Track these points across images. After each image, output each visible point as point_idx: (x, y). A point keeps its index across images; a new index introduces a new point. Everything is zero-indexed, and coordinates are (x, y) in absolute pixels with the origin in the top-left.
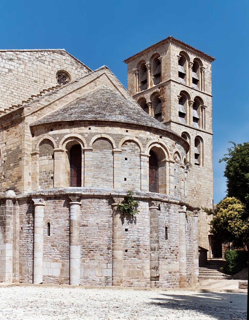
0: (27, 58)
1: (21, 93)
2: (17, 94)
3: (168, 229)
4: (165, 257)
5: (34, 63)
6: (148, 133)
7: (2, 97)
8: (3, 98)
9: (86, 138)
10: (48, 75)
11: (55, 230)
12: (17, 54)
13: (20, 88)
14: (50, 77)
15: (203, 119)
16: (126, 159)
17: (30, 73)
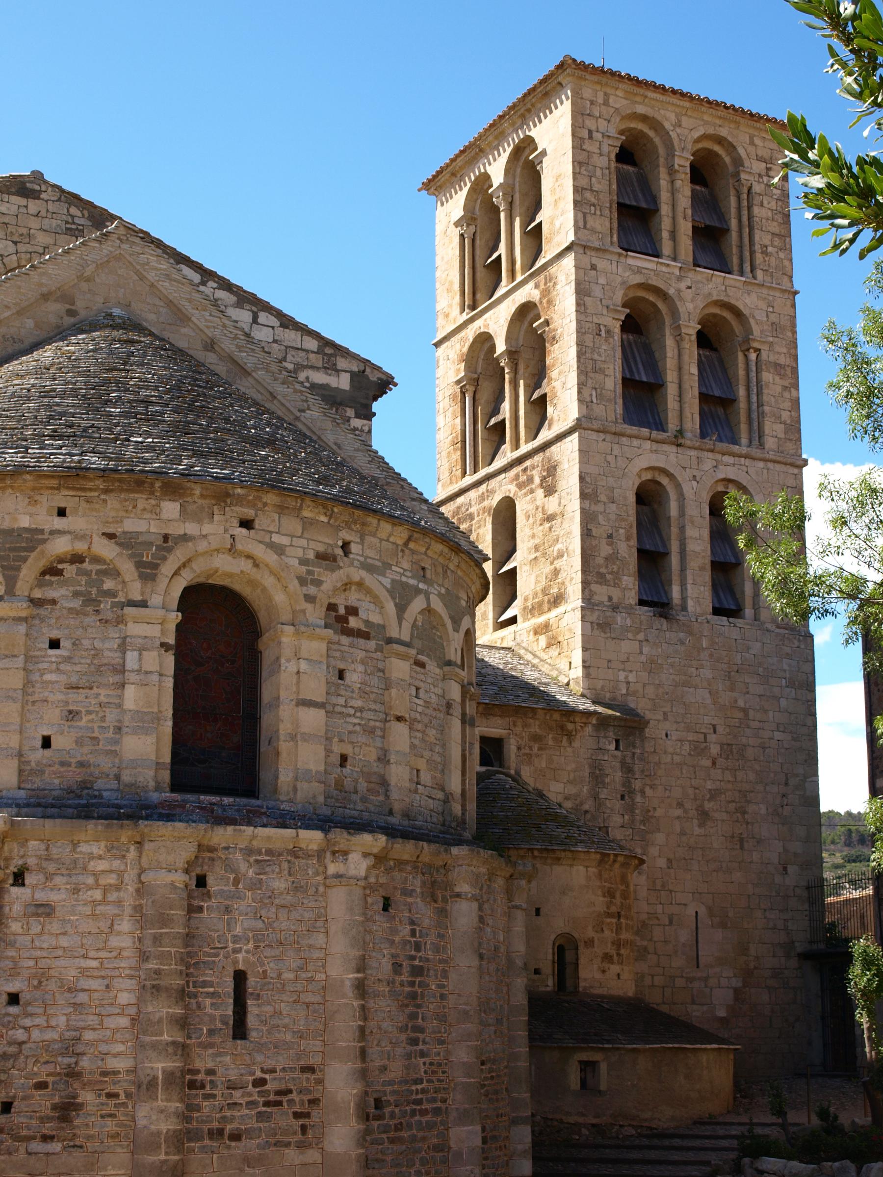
3: (252, 982)
6: (171, 508)
15: (754, 398)
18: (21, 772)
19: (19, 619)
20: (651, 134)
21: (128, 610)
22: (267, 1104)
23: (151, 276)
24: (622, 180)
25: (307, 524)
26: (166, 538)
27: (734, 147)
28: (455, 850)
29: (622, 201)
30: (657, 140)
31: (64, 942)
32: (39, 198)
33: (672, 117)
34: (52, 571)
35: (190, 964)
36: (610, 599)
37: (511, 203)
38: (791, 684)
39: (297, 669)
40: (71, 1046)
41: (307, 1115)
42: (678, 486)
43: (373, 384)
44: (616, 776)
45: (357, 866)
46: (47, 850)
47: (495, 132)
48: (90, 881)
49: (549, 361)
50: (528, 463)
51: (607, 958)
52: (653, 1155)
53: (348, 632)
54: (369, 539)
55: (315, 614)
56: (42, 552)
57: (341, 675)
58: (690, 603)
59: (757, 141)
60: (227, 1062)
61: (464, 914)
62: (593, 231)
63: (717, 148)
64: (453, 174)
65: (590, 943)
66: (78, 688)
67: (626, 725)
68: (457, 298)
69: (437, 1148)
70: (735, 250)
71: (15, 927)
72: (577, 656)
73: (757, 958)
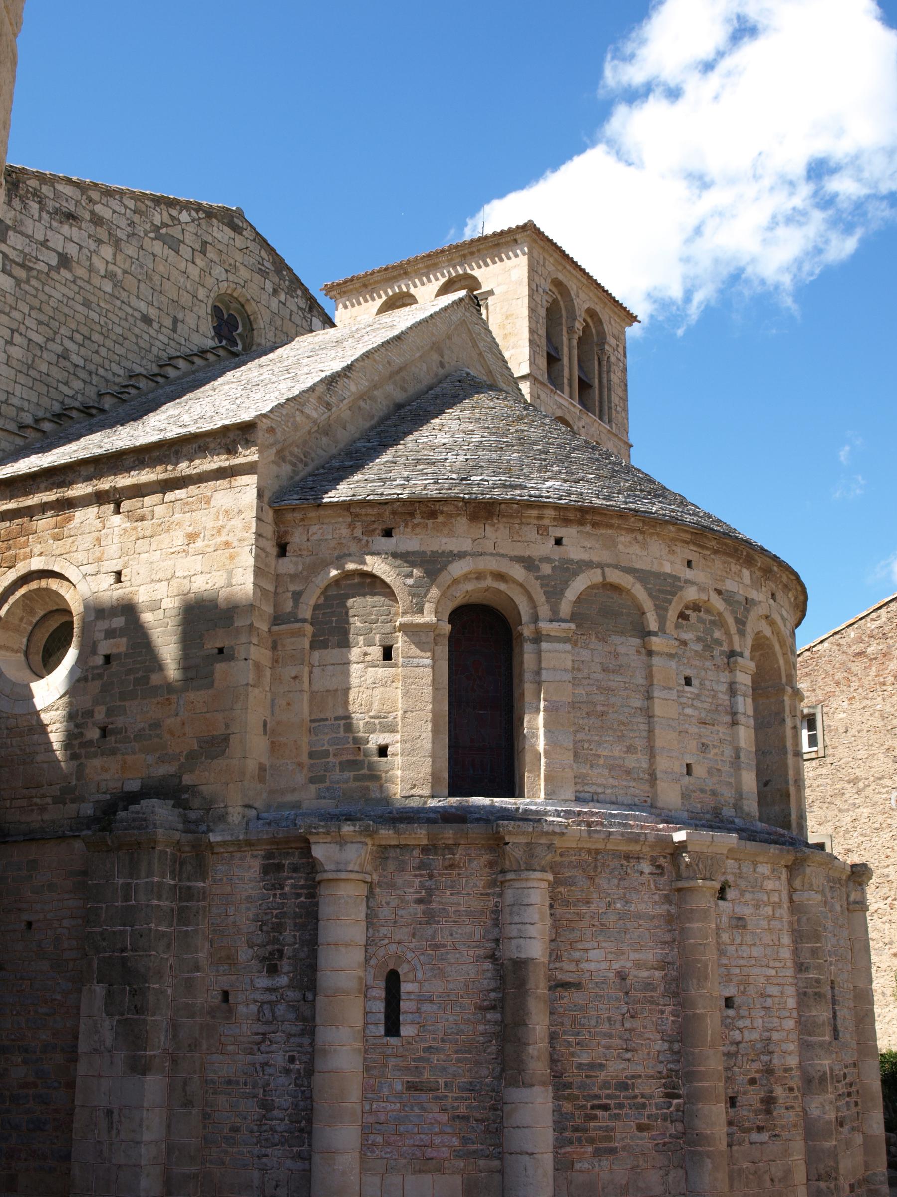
0: (123, 223)
1: (96, 358)
2: (81, 362)
5: (147, 243)
7: (30, 367)
8: (32, 372)
10: (186, 299)
11: (426, 1008)
12: (90, 200)
13: (96, 337)
14: (195, 309)
16: (688, 682)
23: (481, 345)
30: (561, 303)
31: (756, 952)
32: (241, 234)
33: (574, 287)
46: (739, 868)
56: (681, 598)
59: (613, 322)
64: (365, 286)
66: (705, 723)
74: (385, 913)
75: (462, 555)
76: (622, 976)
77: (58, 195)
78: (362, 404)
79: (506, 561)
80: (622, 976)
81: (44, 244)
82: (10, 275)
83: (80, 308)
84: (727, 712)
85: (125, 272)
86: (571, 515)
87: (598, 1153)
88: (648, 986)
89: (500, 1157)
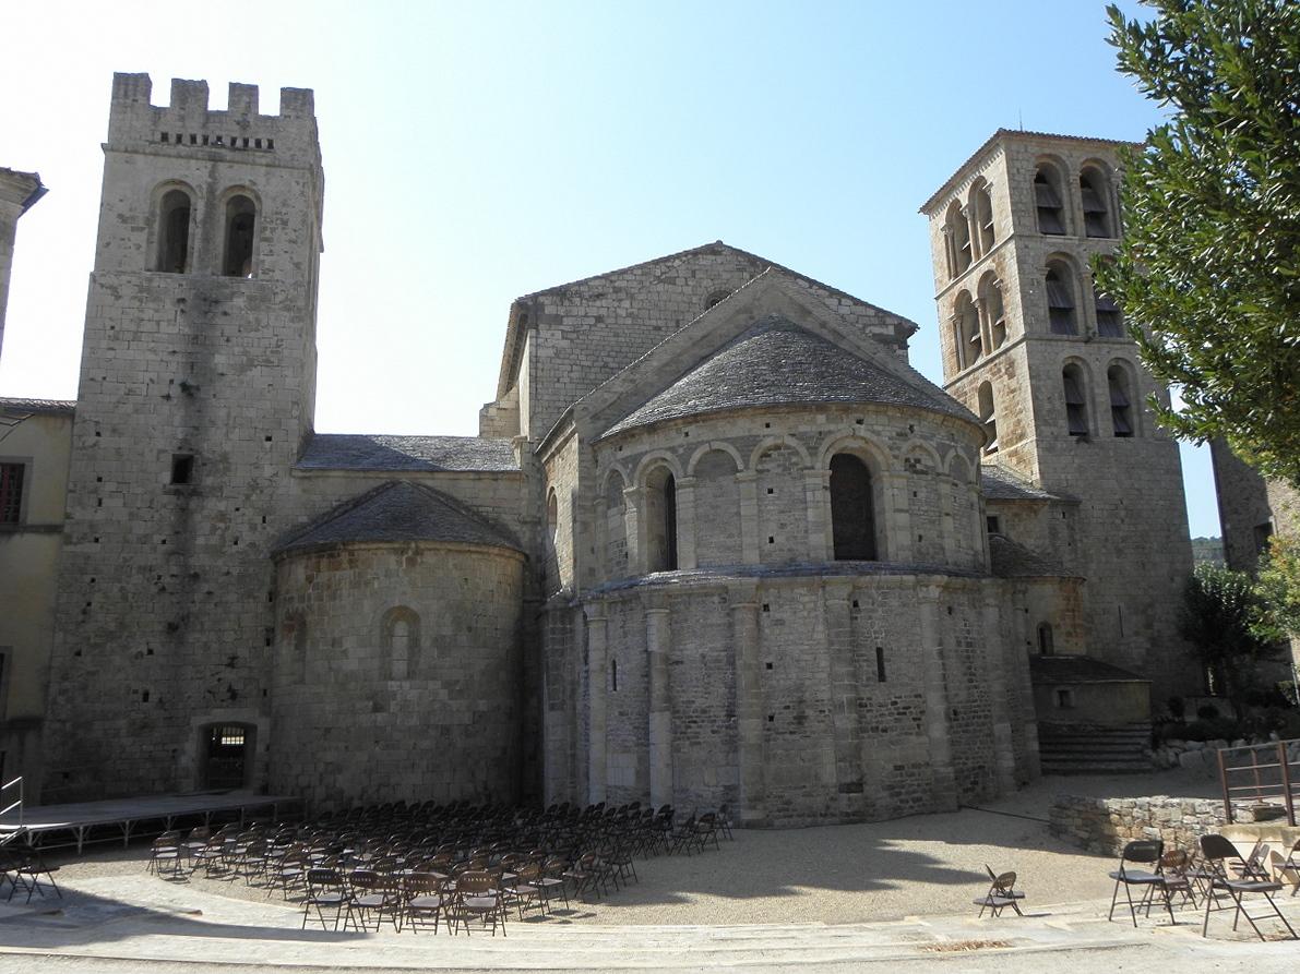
3: (885, 653)
4: (880, 727)
6: (821, 418)
9: (680, 456)
10: (683, 307)
12: (611, 281)
17: (644, 313)
18: (760, 556)
19: (752, 481)
20: (1054, 163)
21: (806, 472)
22: (899, 714)
23: (790, 293)
24: (1039, 193)
25: (891, 419)
26: (820, 433)
27: (1106, 163)
28: (984, 581)
29: (1041, 205)
30: (1058, 167)
31: (791, 637)
33: (1066, 152)
34: (765, 455)
35: (855, 645)
36: (1052, 433)
37: (974, 215)
38: (1167, 472)
39: (893, 497)
40: (800, 688)
41: (919, 719)
42: (1088, 365)
43: (907, 329)
44: (1064, 533)
45: (934, 592)
47: (961, 176)
48: (801, 607)
49: (1004, 303)
50: (997, 361)
51: (1069, 634)
52: (1105, 740)
53: (916, 472)
54: (923, 423)
55: (899, 466)
57: (915, 494)
58: (1101, 431)
60: (878, 694)
61: (991, 614)
62: (1025, 226)
63: (1096, 166)
65: (1058, 626)
67: (1068, 504)
68: (947, 271)
69: (989, 735)
70: (1111, 224)
71: (767, 631)
72: (1036, 468)
73: (1159, 631)
74: (611, 633)
75: (646, 452)
76: (703, 656)
77: (590, 288)
78: (668, 369)
79: (663, 451)
80: (703, 656)
81: (586, 316)
82: (566, 339)
83: (612, 339)
84: (802, 502)
85: (639, 309)
86: (690, 420)
87: (692, 744)
88: (717, 661)
89: (648, 745)
